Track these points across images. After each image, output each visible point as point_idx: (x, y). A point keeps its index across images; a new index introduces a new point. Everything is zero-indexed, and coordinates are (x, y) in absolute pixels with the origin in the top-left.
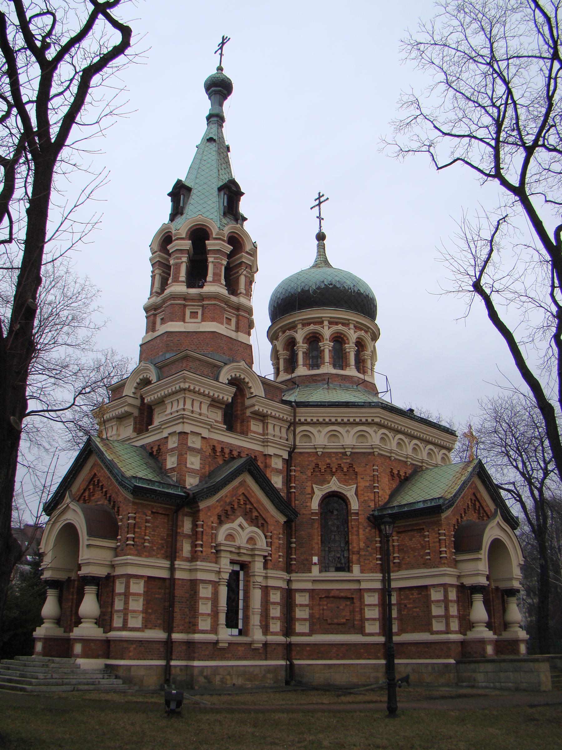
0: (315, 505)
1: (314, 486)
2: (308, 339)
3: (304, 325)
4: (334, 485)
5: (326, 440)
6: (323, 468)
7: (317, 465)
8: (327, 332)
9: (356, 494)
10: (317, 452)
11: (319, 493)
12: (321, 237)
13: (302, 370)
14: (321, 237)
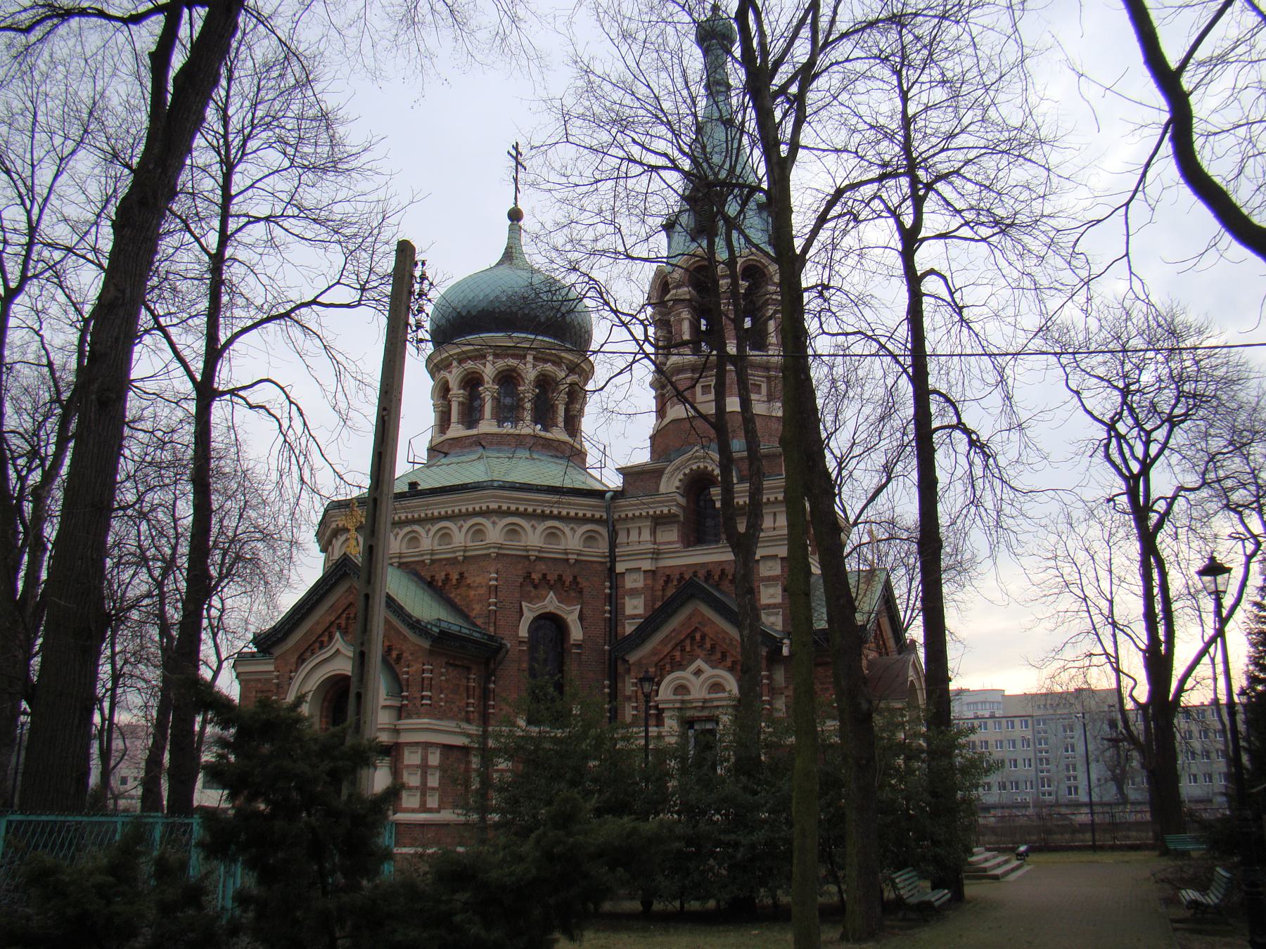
0: (523, 632)
1: (524, 604)
2: (500, 380)
3: (496, 356)
4: (551, 603)
5: (542, 540)
6: (536, 577)
7: (528, 576)
8: (530, 372)
9: (581, 617)
10: (528, 556)
11: (528, 616)
12: (515, 215)
13: (487, 426)
14: (515, 215)
